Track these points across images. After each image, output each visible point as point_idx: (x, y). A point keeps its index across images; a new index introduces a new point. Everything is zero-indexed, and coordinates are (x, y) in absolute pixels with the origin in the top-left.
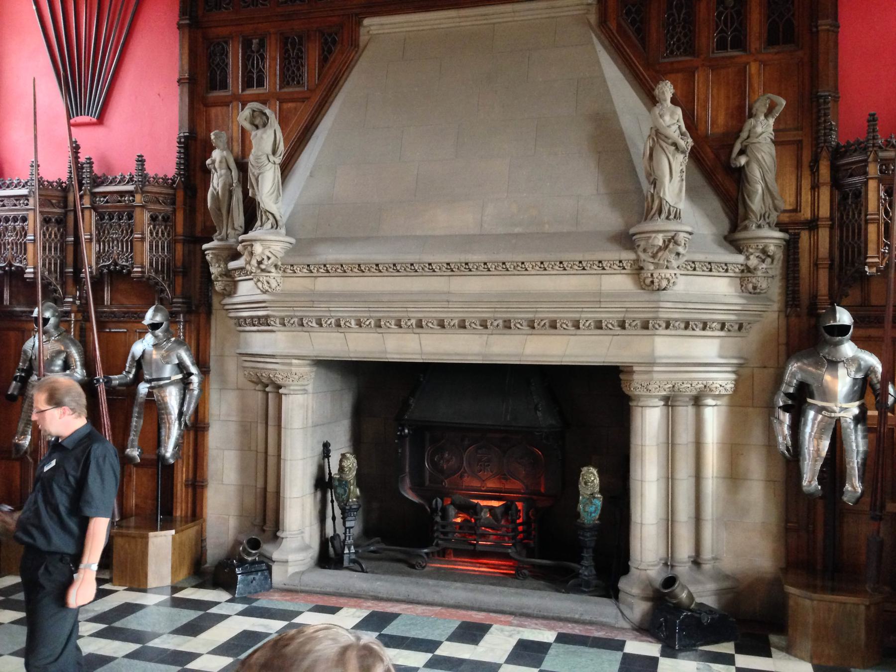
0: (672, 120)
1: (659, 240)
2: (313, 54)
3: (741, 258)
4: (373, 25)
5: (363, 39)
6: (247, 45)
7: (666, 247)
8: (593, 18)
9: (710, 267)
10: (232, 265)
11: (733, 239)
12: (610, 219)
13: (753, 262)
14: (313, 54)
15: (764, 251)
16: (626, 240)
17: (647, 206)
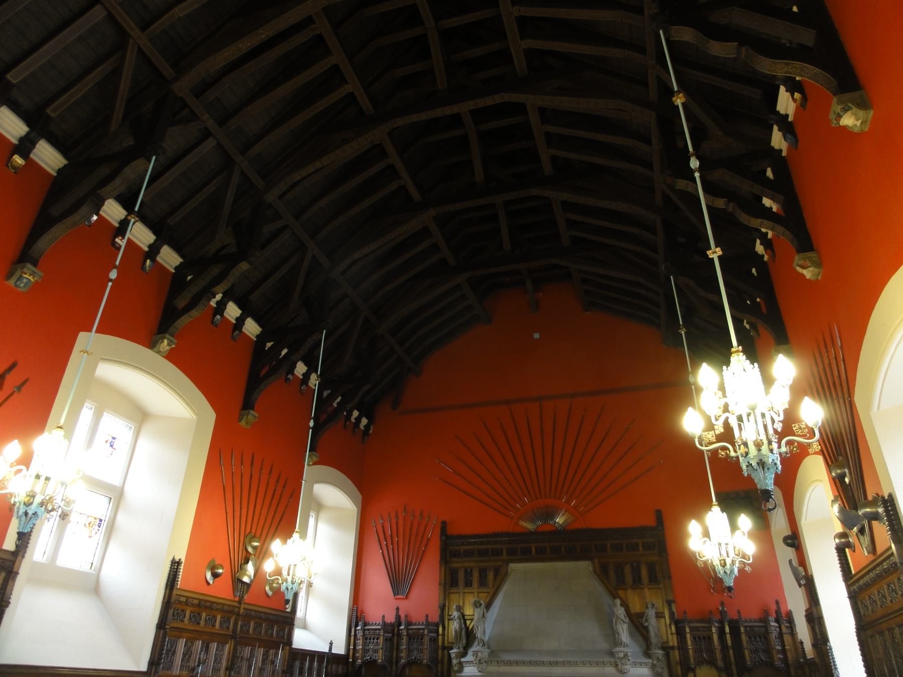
0: (621, 612)
1: (622, 655)
2: (491, 575)
3: (650, 661)
4: (512, 566)
5: (509, 571)
6: (466, 571)
7: (624, 657)
8: (591, 568)
9: (641, 664)
10: (463, 660)
11: (647, 654)
12: (604, 645)
13: (655, 662)
14: (491, 575)
15: (658, 658)
16: (611, 654)
17: (617, 643)
